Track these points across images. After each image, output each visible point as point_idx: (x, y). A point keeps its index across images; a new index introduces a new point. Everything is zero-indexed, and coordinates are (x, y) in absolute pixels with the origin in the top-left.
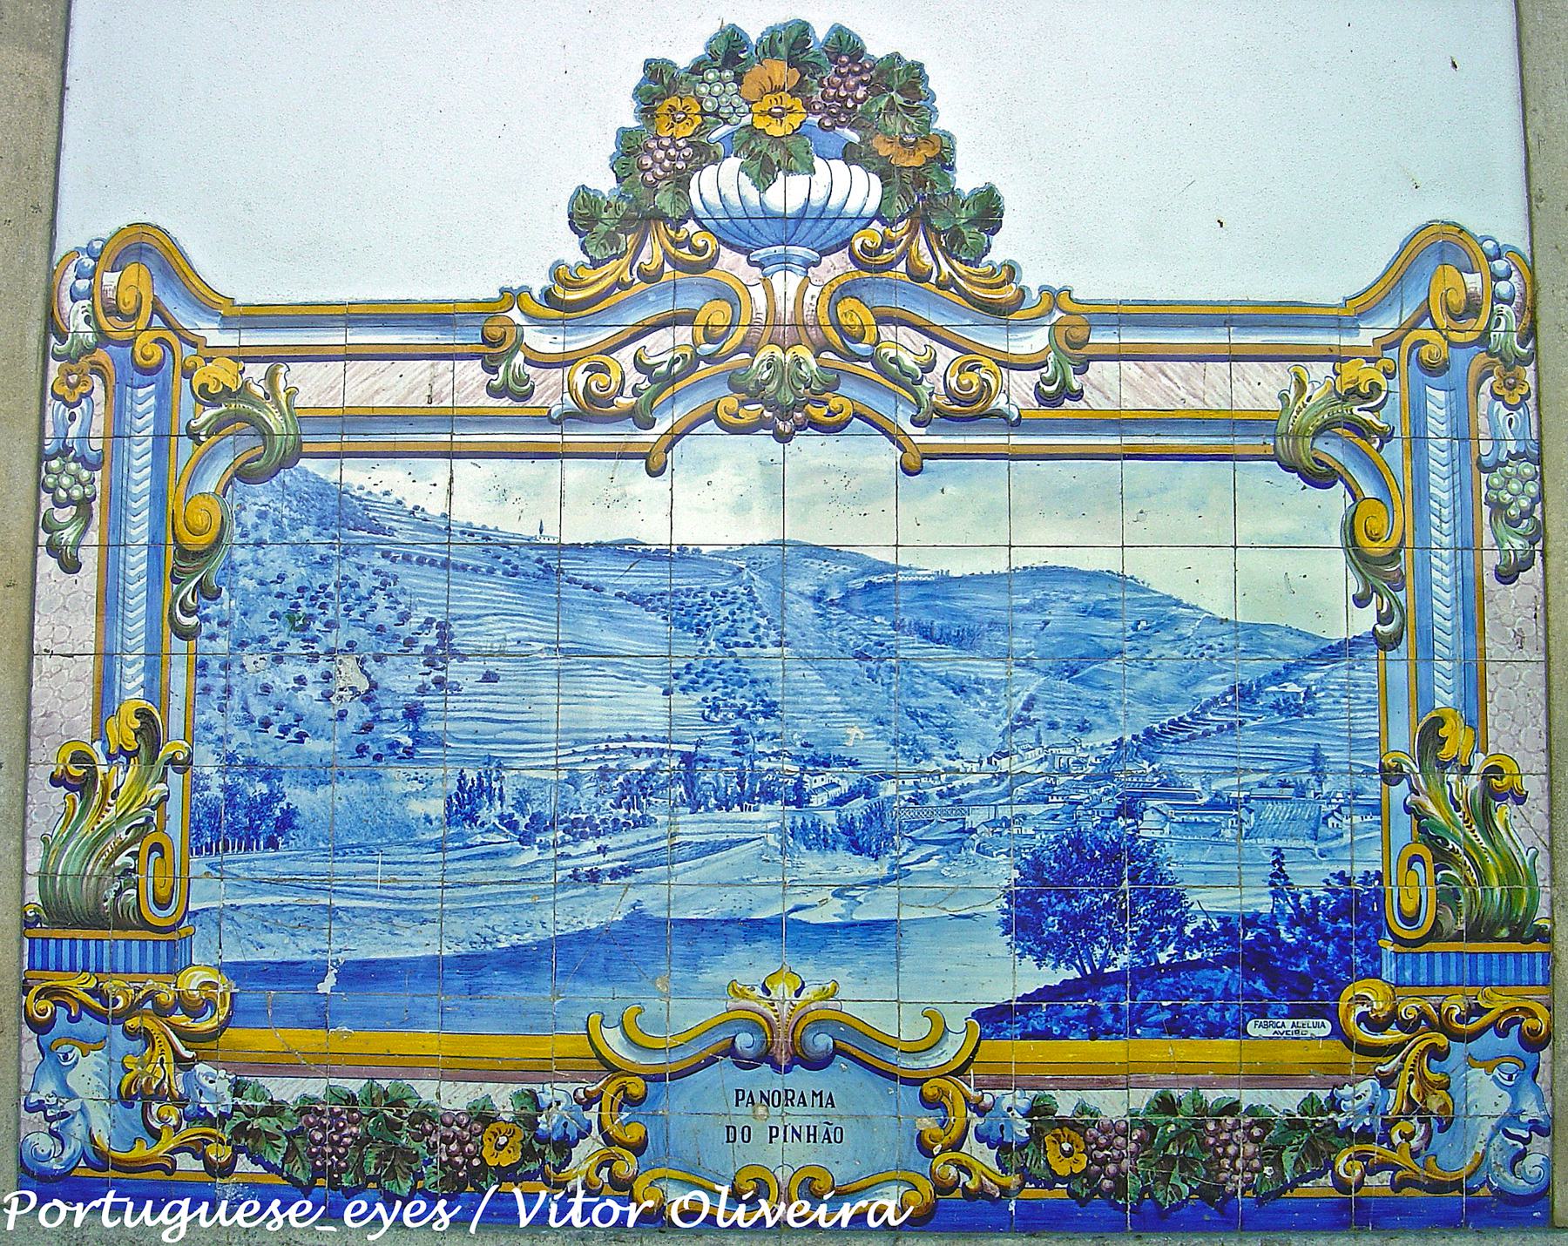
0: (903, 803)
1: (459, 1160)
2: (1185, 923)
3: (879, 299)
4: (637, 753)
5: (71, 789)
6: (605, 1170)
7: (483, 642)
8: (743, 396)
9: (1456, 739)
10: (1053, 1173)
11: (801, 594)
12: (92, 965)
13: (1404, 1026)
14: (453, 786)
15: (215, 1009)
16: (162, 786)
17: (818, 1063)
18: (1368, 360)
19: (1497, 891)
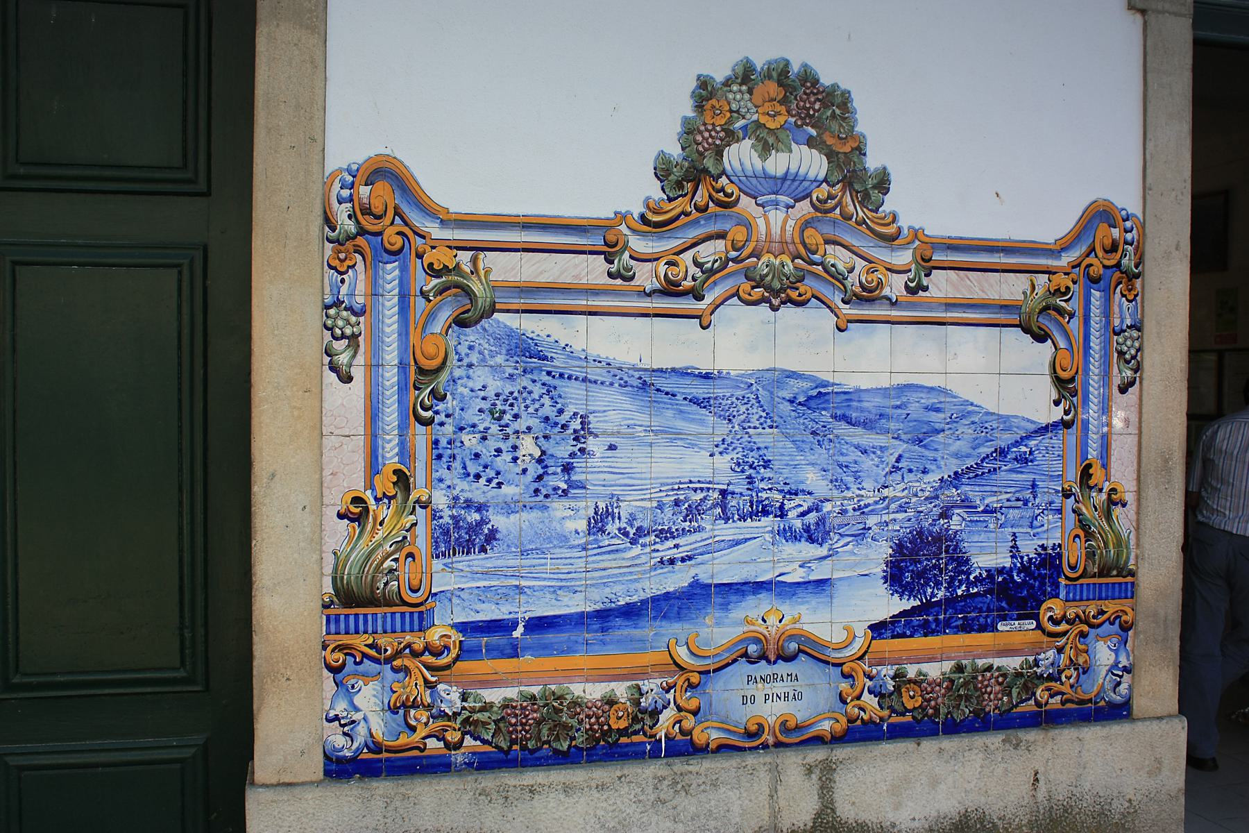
0: (835, 514)
1: (596, 727)
2: (970, 574)
3: (828, 230)
4: (695, 490)
5: (352, 520)
6: (678, 725)
7: (609, 427)
8: (753, 284)
9: (1097, 474)
10: (905, 708)
11: (784, 398)
12: (370, 631)
13: (1068, 622)
14: (591, 512)
15: (449, 650)
16: (412, 517)
18: (1065, 274)
19: (1112, 552)
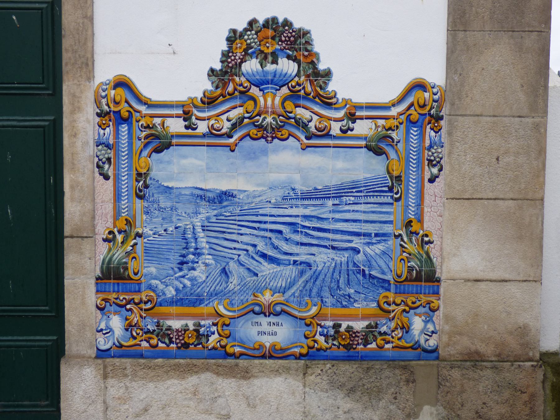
6: (218, 344)
17: (277, 314)
